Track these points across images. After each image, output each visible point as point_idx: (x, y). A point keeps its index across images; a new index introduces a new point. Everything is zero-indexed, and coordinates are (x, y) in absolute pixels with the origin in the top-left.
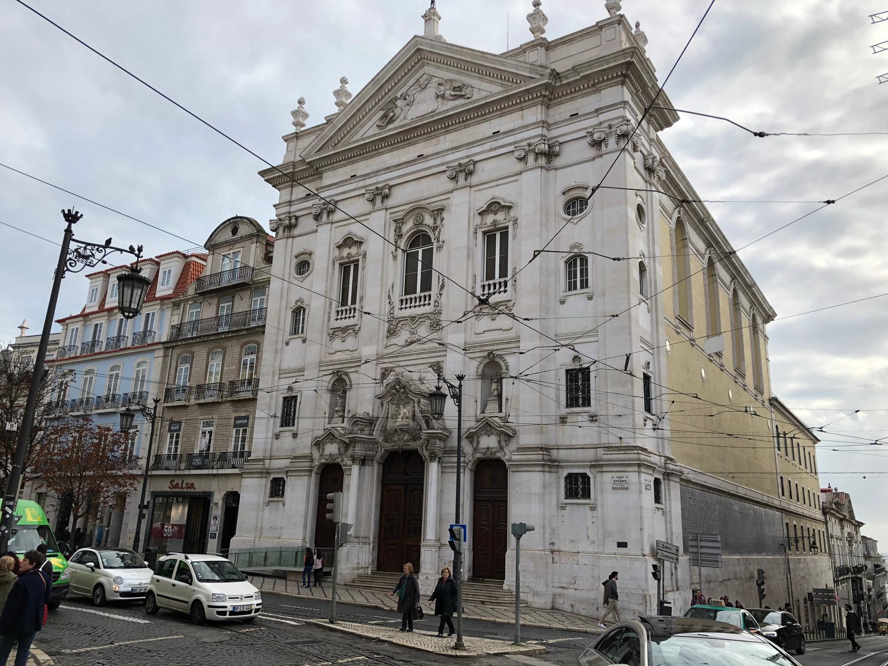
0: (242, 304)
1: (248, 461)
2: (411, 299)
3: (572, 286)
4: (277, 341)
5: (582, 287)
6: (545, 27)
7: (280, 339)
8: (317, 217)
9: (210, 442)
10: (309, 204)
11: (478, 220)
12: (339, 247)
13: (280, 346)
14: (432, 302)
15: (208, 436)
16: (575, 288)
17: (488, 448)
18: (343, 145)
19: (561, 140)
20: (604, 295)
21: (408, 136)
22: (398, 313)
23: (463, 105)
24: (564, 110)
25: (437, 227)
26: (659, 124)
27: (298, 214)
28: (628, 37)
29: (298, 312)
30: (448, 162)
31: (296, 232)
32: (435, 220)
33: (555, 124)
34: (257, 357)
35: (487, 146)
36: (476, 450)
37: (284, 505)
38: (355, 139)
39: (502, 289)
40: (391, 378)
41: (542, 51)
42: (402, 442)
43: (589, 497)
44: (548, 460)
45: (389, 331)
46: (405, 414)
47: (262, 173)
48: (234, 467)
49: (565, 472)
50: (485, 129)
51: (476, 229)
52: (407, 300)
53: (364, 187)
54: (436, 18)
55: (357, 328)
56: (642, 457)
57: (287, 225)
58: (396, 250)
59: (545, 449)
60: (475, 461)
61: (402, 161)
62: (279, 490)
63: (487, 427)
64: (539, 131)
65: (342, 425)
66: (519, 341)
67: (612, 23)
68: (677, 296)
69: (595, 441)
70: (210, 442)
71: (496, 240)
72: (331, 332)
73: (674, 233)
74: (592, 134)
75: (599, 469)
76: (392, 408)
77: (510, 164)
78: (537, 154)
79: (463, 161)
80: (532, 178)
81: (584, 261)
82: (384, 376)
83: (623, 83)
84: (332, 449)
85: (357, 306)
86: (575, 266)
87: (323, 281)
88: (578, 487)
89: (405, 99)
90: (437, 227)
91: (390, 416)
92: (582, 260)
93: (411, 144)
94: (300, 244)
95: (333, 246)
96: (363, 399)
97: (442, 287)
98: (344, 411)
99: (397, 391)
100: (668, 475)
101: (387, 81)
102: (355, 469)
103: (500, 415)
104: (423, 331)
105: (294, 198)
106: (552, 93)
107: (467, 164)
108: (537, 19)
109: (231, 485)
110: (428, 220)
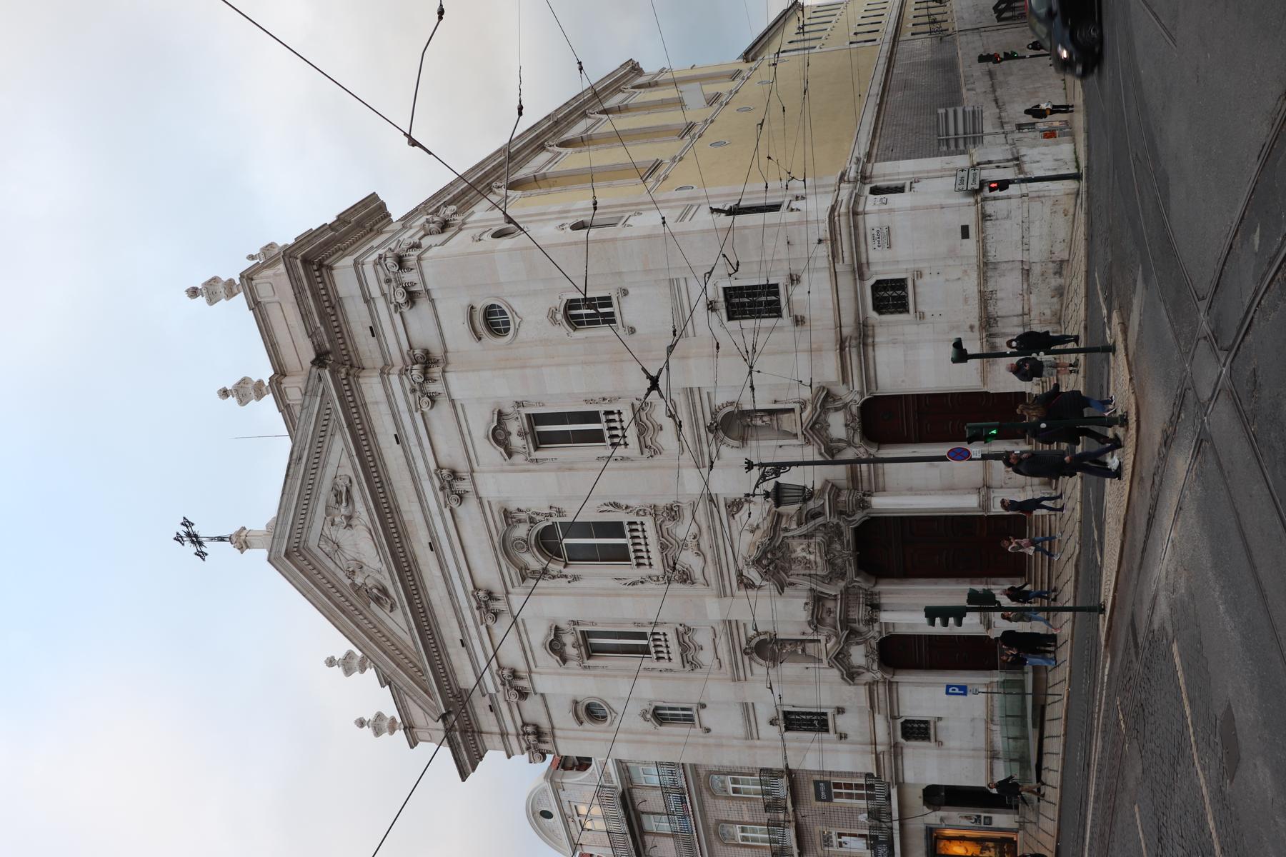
0: (651, 800)
1: (879, 777)
2: (635, 551)
3: (609, 319)
4: (705, 745)
5: (610, 305)
6: (255, 380)
7: (701, 740)
8: (523, 694)
9: (855, 835)
10: (504, 707)
11: (518, 459)
12: (564, 660)
13: (711, 741)
14: (638, 520)
15: (844, 839)
16: (612, 314)
17: (846, 425)
18: (421, 660)
19: (405, 347)
20: (620, 274)
21: (405, 566)
22: (658, 569)
23: (361, 489)
24: (365, 345)
25: (531, 518)
26: (383, 219)
27: (519, 723)
28: (268, 267)
29: (660, 716)
30: (439, 506)
31: (545, 725)
32: (520, 521)
33: (384, 357)
34: (728, 774)
35: (416, 451)
36: (849, 443)
37: (940, 719)
38: (410, 643)
39: (616, 417)
40: (753, 574)
41: (287, 382)
42: (845, 552)
43: (903, 281)
44: (856, 343)
45: (685, 581)
46: (803, 550)
47: (464, 776)
48: (889, 798)
49: (873, 315)
50: (392, 455)
51: (532, 460)
52: (637, 558)
53: (477, 628)
54: (244, 533)
55: (681, 629)
56: (843, 210)
57: (536, 739)
59: (842, 344)
60: (867, 444)
61: (439, 573)
62: (919, 728)
63: (816, 429)
64: (394, 379)
65: (823, 642)
66: (691, 389)
67: (251, 290)
68: (615, 182)
69: (825, 276)
70: (855, 835)
71: (547, 431)
73: (528, 192)
74: (398, 306)
75: (865, 269)
76: (797, 569)
77: (441, 417)
78: (426, 379)
79: (437, 484)
80: (459, 383)
81: (571, 304)
82: (750, 585)
83: (330, 268)
84: (858, 655)
85: (648, 630)
86: (580, 316)
87: (612, 682)
88: (891, 296)
89: (353, 572)
90: (531, 518)
91: (807, 572)
92: (572, 308)
93: (415, 561)
94: (563, 718)
95: (562, 670)
96: (786, 613)
97: (616, 505)
98: (802, 641)
99: (773, 562)
100: (864, 178)
101: (330, 599)
102: (885, 617)
104: (682, 530)
105: (497, 730)
106: (343, 364)
107: (441, 479)
108: (244, 391)
109: (915, 798)
110: (521, 531)
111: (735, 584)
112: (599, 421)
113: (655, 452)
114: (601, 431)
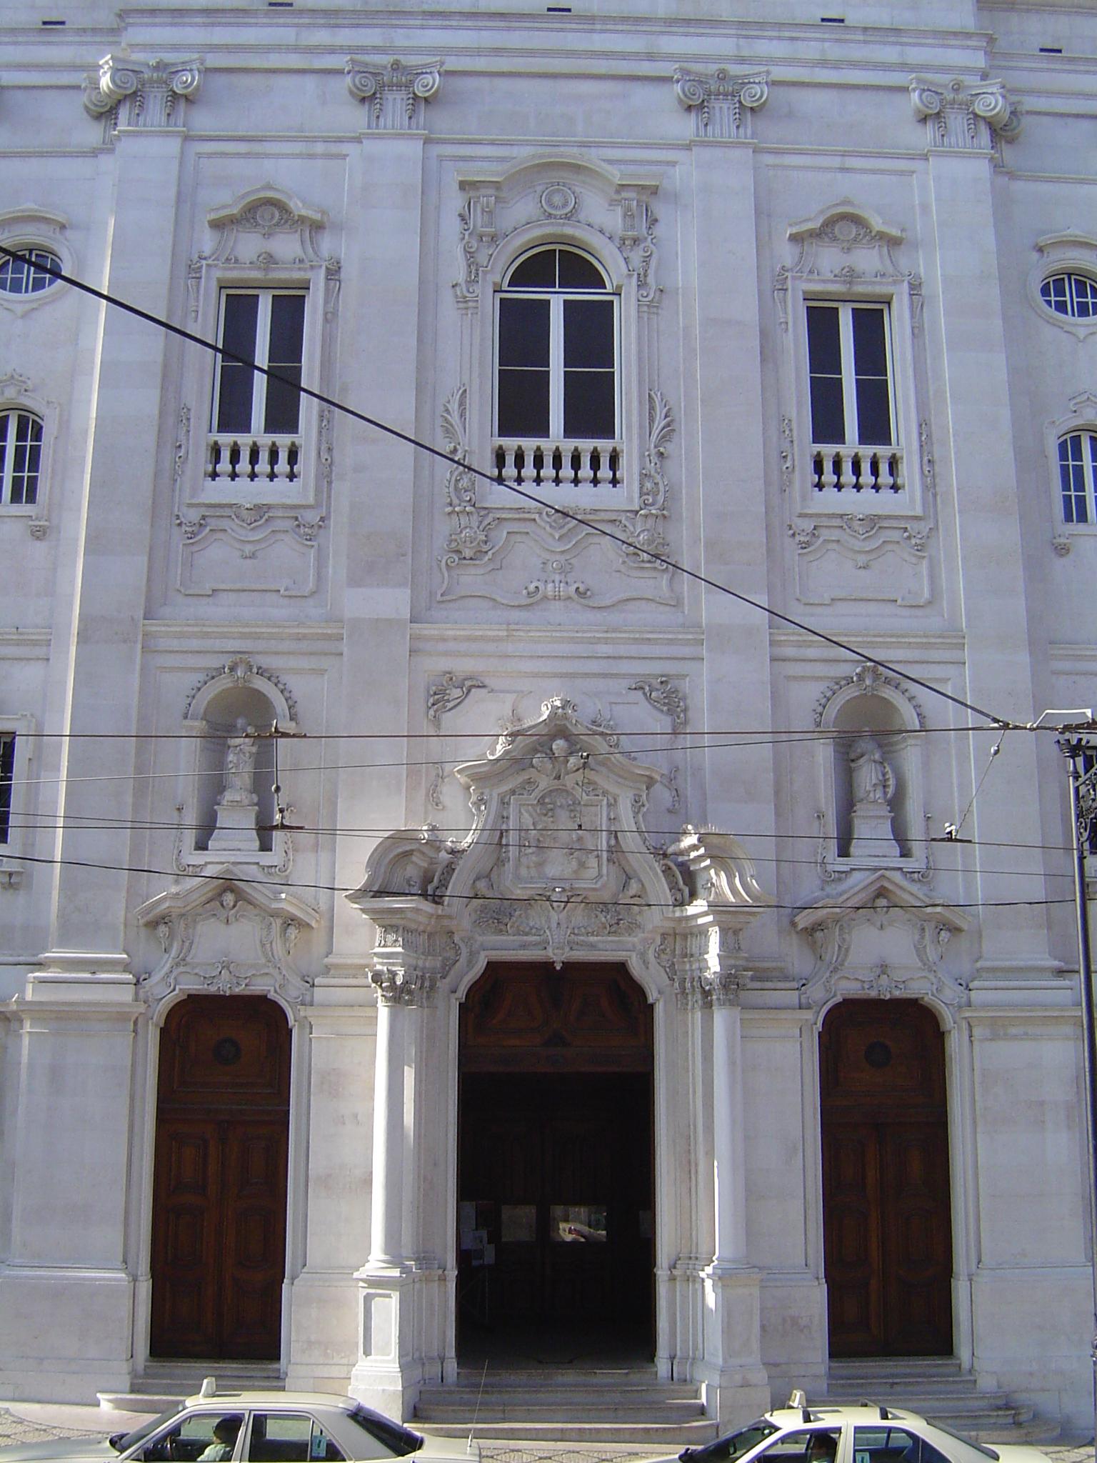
35: (810, 49)
53: (350, 50)
58: (471, 282)
72: (193, 515)
86: (1078, 455)
97: (668, 433)
111: (444, 664)
112: (864, 439)
114: (839, 438)
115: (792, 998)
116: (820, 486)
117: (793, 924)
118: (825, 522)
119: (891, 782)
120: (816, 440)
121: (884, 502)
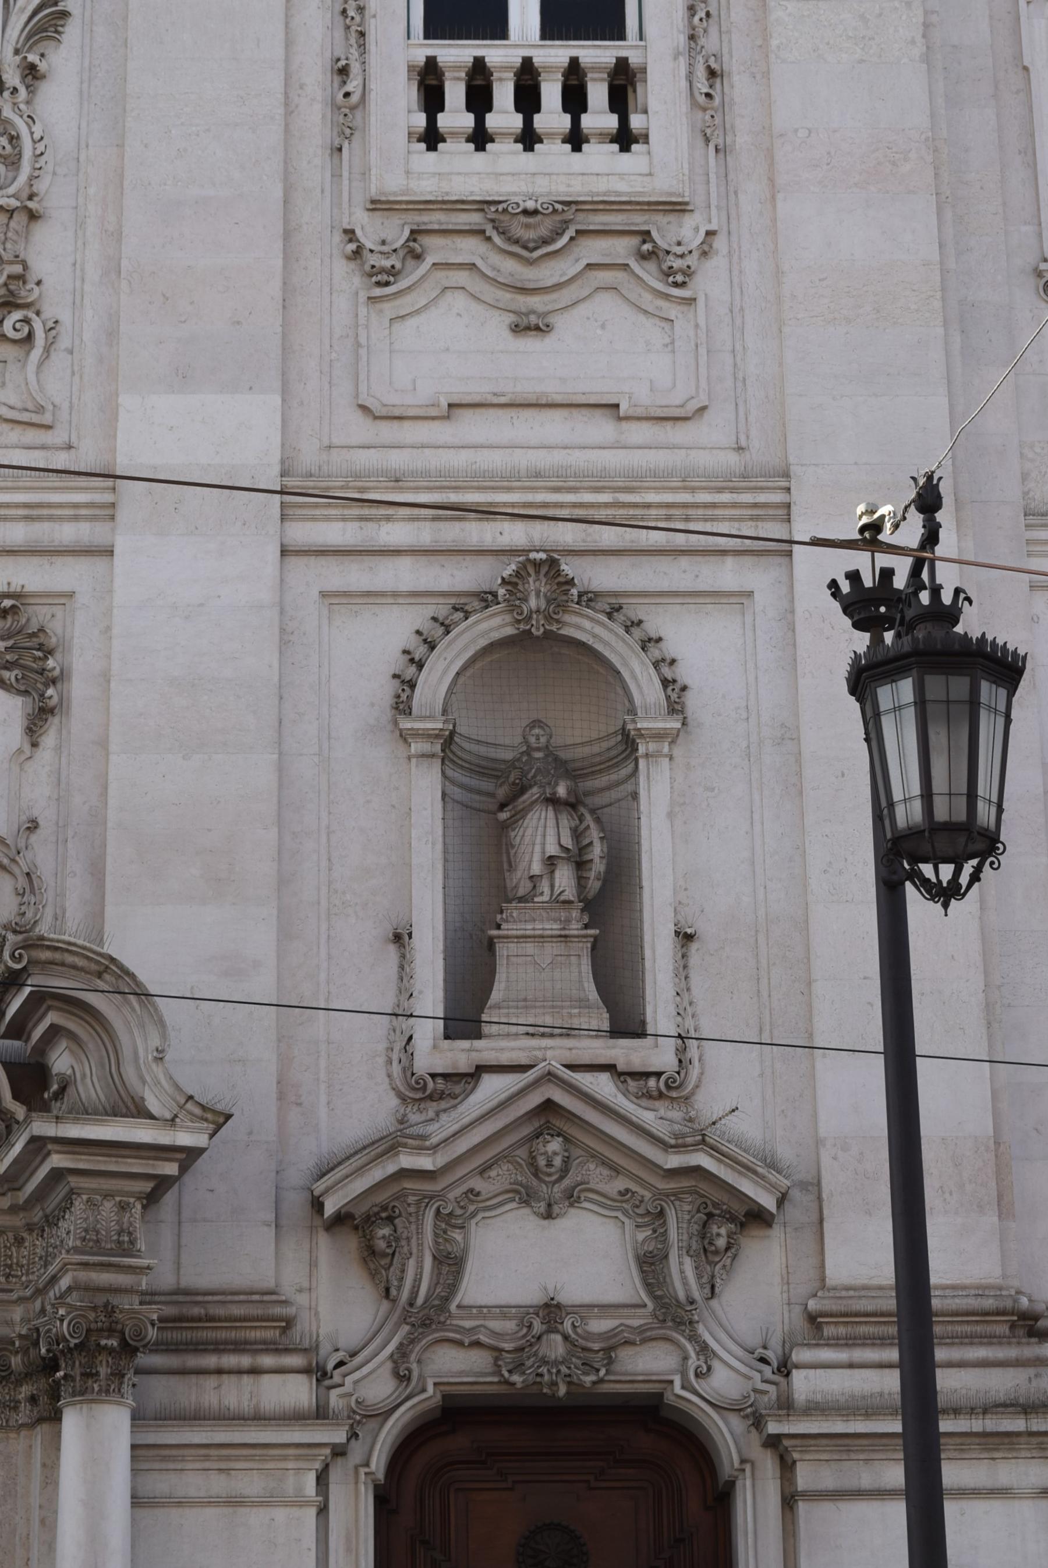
103: (626, 1052)
113: (383, 278)
115: (297, 1392)
116: (432, 138)
117: (317, 1205)
118: (435, 219)
119: (597, 851)
120: (430, 32)
121: (601, 171)
